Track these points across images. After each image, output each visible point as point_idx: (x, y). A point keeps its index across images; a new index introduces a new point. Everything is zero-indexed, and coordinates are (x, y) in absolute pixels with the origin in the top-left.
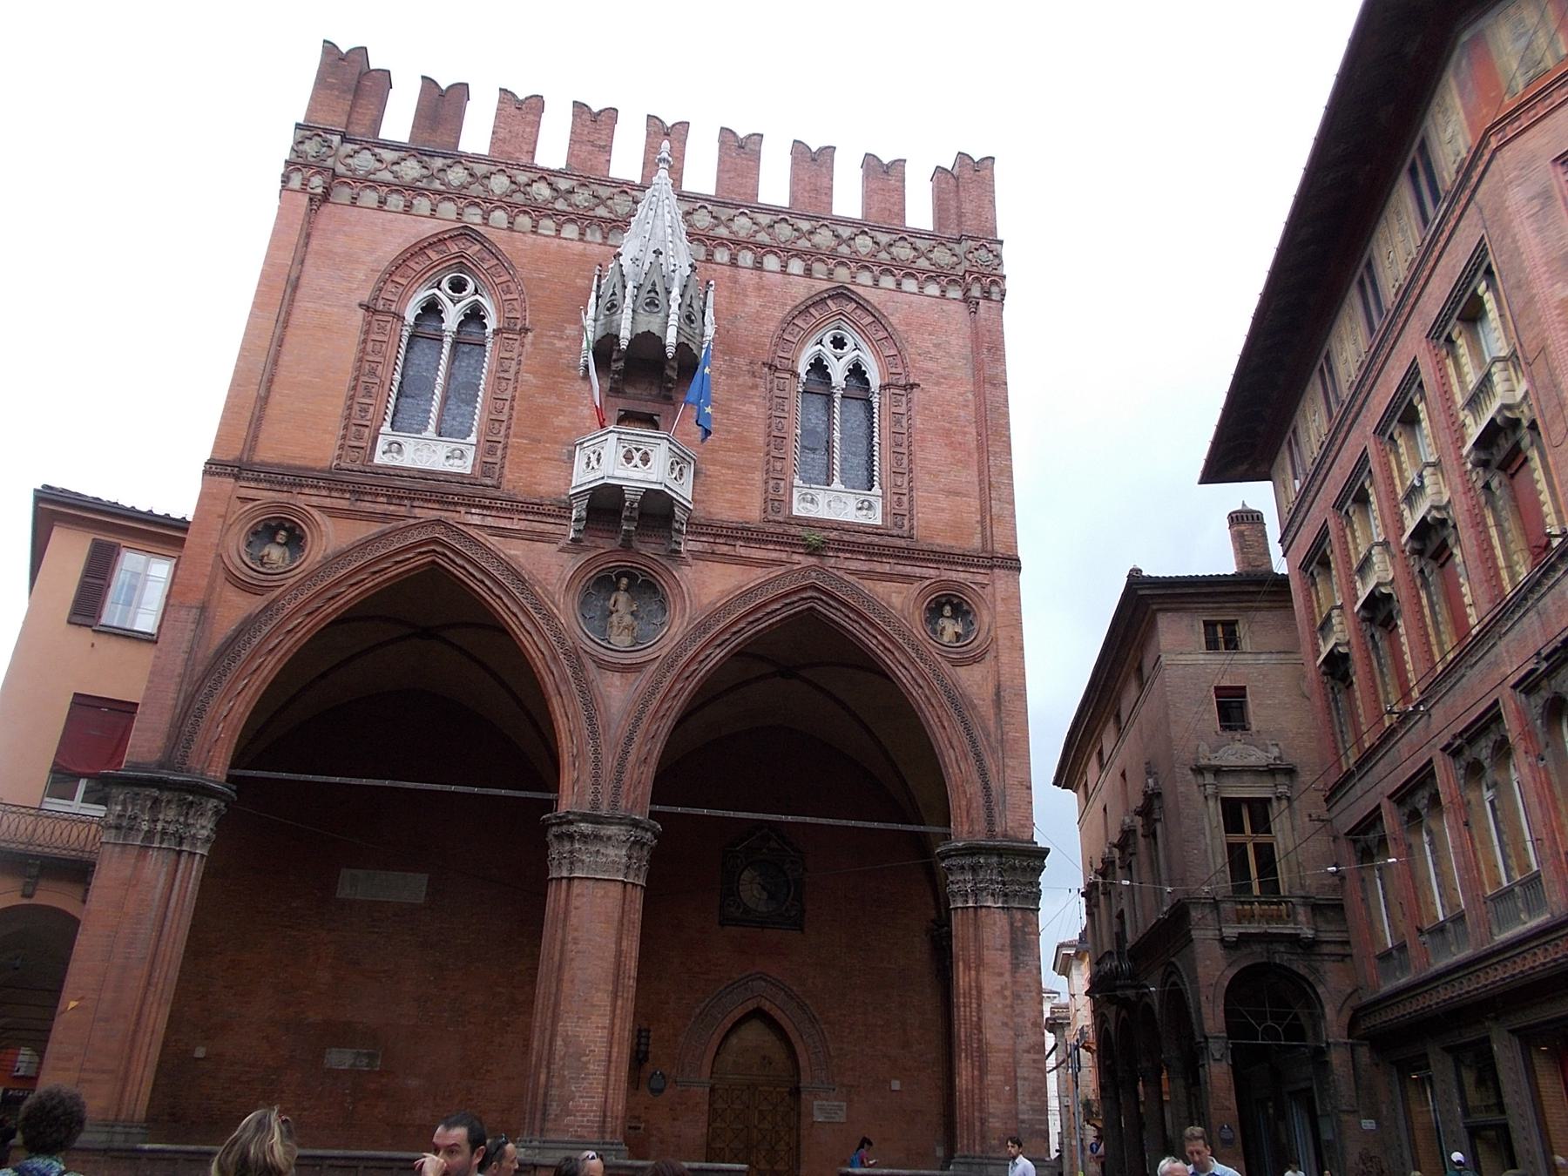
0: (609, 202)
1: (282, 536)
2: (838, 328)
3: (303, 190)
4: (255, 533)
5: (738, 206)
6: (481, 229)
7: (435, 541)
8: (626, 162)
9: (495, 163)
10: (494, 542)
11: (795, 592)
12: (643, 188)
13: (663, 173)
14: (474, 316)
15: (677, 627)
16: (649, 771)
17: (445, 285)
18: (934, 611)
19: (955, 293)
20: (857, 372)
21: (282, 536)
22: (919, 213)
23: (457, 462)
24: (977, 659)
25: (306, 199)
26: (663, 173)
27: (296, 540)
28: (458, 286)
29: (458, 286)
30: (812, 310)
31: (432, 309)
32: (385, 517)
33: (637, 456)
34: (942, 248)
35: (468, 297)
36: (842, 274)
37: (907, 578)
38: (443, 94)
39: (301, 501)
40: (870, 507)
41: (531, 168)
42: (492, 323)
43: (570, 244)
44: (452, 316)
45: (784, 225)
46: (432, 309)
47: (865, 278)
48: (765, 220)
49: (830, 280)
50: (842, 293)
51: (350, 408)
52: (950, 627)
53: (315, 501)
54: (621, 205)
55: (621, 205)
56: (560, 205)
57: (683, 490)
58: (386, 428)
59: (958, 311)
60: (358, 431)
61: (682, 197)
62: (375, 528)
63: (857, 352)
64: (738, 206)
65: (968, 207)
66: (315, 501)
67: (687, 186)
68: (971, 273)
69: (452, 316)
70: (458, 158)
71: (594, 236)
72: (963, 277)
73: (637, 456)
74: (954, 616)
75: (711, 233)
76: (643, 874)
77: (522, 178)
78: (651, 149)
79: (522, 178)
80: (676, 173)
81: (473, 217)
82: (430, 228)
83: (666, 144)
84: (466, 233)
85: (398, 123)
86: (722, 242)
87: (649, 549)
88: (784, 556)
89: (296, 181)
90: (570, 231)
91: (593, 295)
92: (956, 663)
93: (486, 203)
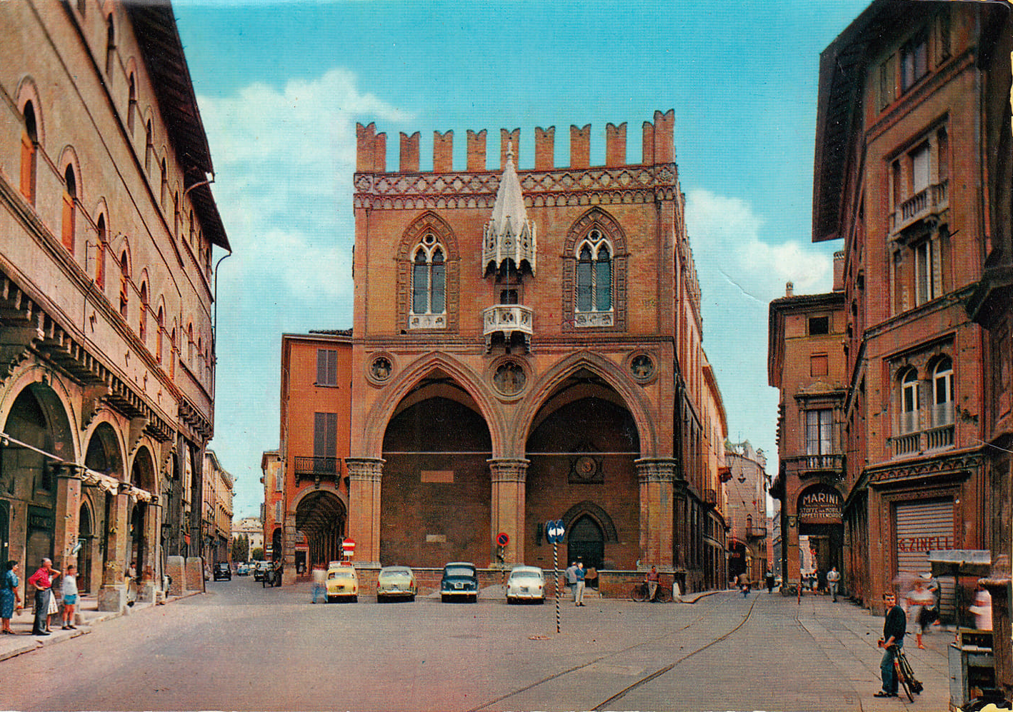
0: (488, 184)
1: (383, 365)
2: (595, 228)
3: (363, 207)
4: (374, 365)
5: (545, 172)
6: (436, 211)
7: (437, 359)
8: (492, 162)
9: (436, 174)
10: (460, 358)
11: (577, 362)
12: (501, 172)
13: (510, 162)
14: (438, 252)
15: (529, 385)
16: (524, 441)
17: (424, 240)
18: (636, 362)
19: (650, 199)
20: (604, 248)
21: (383, 365)
22: (634, 154)
23: (441, 323)
24: (654, 381)
25: (363, 211)
26: (510, 162)
27: (387, 366)
28: (429, 240)
29: (429, 240)
30: (582, 223)
31: (421, 252)
32: (418, 353)
33: (508, 317)
34: (645, 174)
35: (435, 244)
36: (595, 201)
37: (622, 350)
38: (410, 140)
39: (387, 350)
40: (609, 318)
41: (452, 173)
42: (445, 255)
43: (473, 211)
44: (429, 254)
45: (567, 177)
46: (421, 252)
47: (606, 199)
48: (557, 177)
49: (589, 204)
50: (596, 210)
51: (397, 307)
52: (642, 369)
53: (392, 349)
54: (493, 185)
55: (493, 185)
56: (467, 191)
57: (527, 328)
58: (412, 313)
59: (650, 208)
60: (401, 316)
61: (519, 173)
62: (416, 357)
63: (603, 240)
64: (545, 172)
65: (658, 145)
66: (392, 349)
67: (522, 167)
68: (658, 186)
69: (429, 254)
70: (421, 175)
71: (482, 204)
72: (654, 189)
73: (508, 317)
74: (644, 364)
75: (533, 191)
76: (524, 478)
77: (449, 179)
78: (504, 149)
79: (449, 179)
80: (516, 159)
81: (430, 205)
82: (414, 215)
83: (510, 144)
84: (430, 213)
85: (392, 163)
86: (538, 194)
87: (517, 351)
88: (571, 348)
89: (359, 205)
90: (472, 204)
91: (484, 241)
92: (642, 385)
93: (435, 197)
